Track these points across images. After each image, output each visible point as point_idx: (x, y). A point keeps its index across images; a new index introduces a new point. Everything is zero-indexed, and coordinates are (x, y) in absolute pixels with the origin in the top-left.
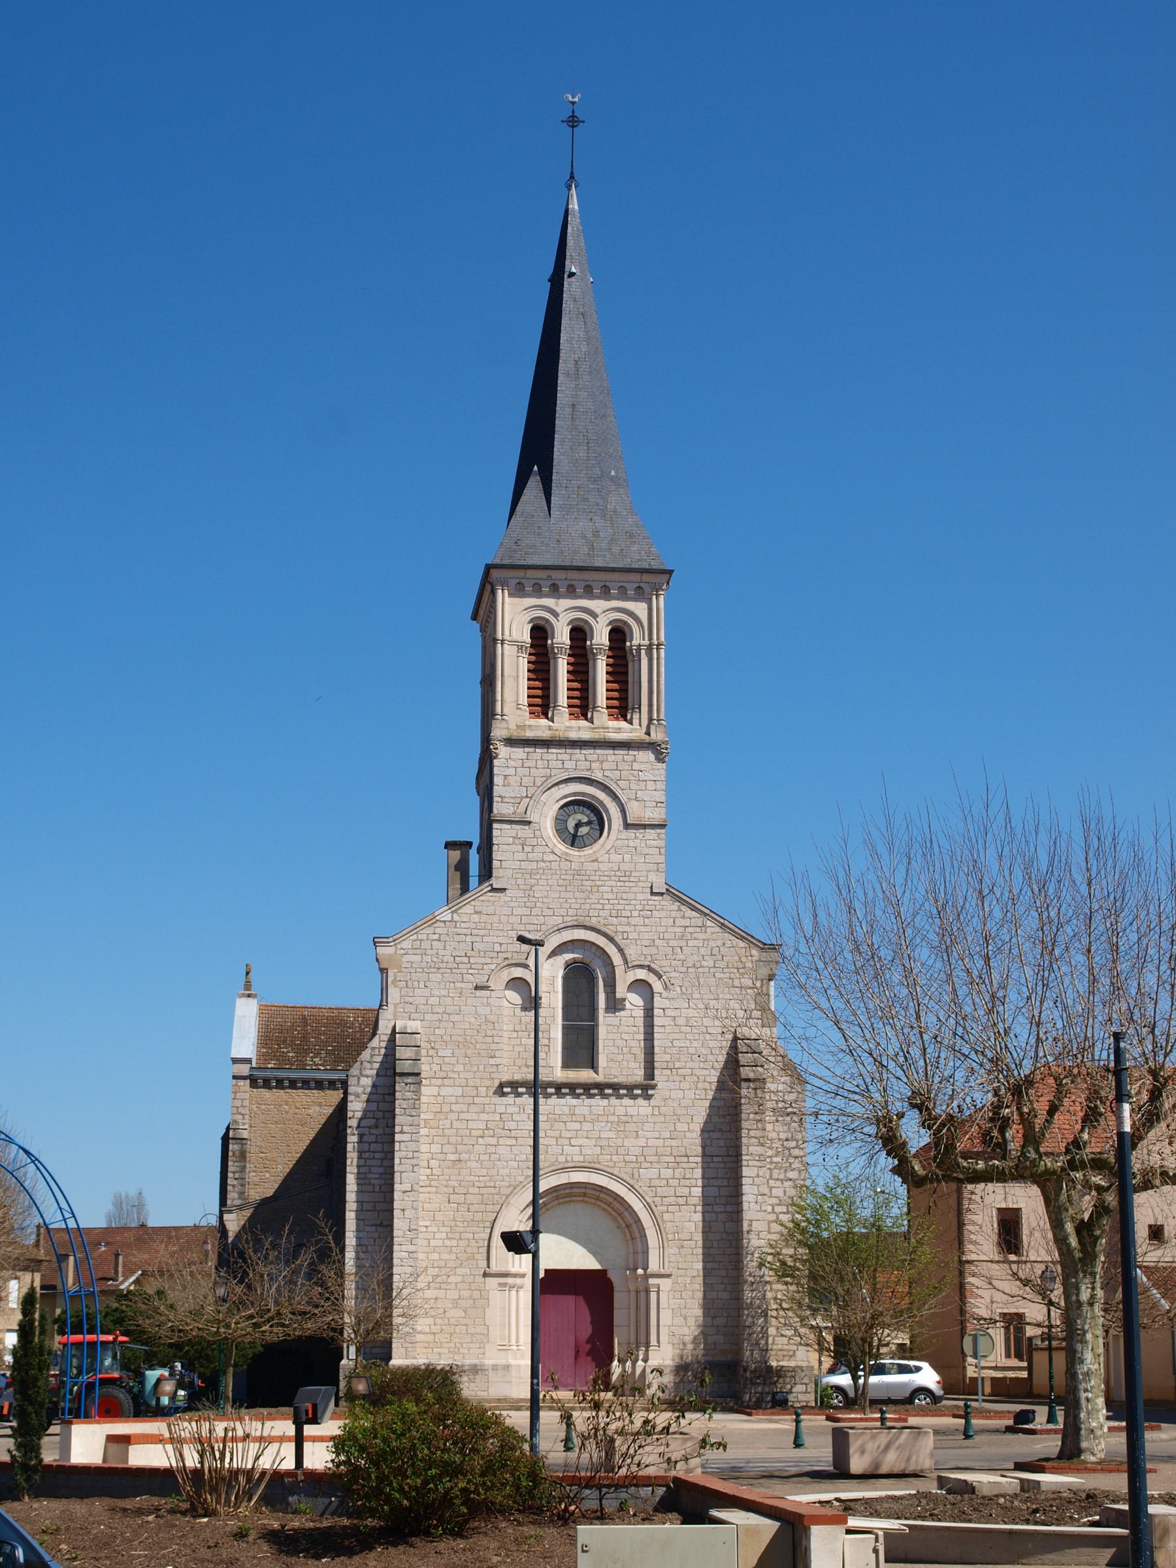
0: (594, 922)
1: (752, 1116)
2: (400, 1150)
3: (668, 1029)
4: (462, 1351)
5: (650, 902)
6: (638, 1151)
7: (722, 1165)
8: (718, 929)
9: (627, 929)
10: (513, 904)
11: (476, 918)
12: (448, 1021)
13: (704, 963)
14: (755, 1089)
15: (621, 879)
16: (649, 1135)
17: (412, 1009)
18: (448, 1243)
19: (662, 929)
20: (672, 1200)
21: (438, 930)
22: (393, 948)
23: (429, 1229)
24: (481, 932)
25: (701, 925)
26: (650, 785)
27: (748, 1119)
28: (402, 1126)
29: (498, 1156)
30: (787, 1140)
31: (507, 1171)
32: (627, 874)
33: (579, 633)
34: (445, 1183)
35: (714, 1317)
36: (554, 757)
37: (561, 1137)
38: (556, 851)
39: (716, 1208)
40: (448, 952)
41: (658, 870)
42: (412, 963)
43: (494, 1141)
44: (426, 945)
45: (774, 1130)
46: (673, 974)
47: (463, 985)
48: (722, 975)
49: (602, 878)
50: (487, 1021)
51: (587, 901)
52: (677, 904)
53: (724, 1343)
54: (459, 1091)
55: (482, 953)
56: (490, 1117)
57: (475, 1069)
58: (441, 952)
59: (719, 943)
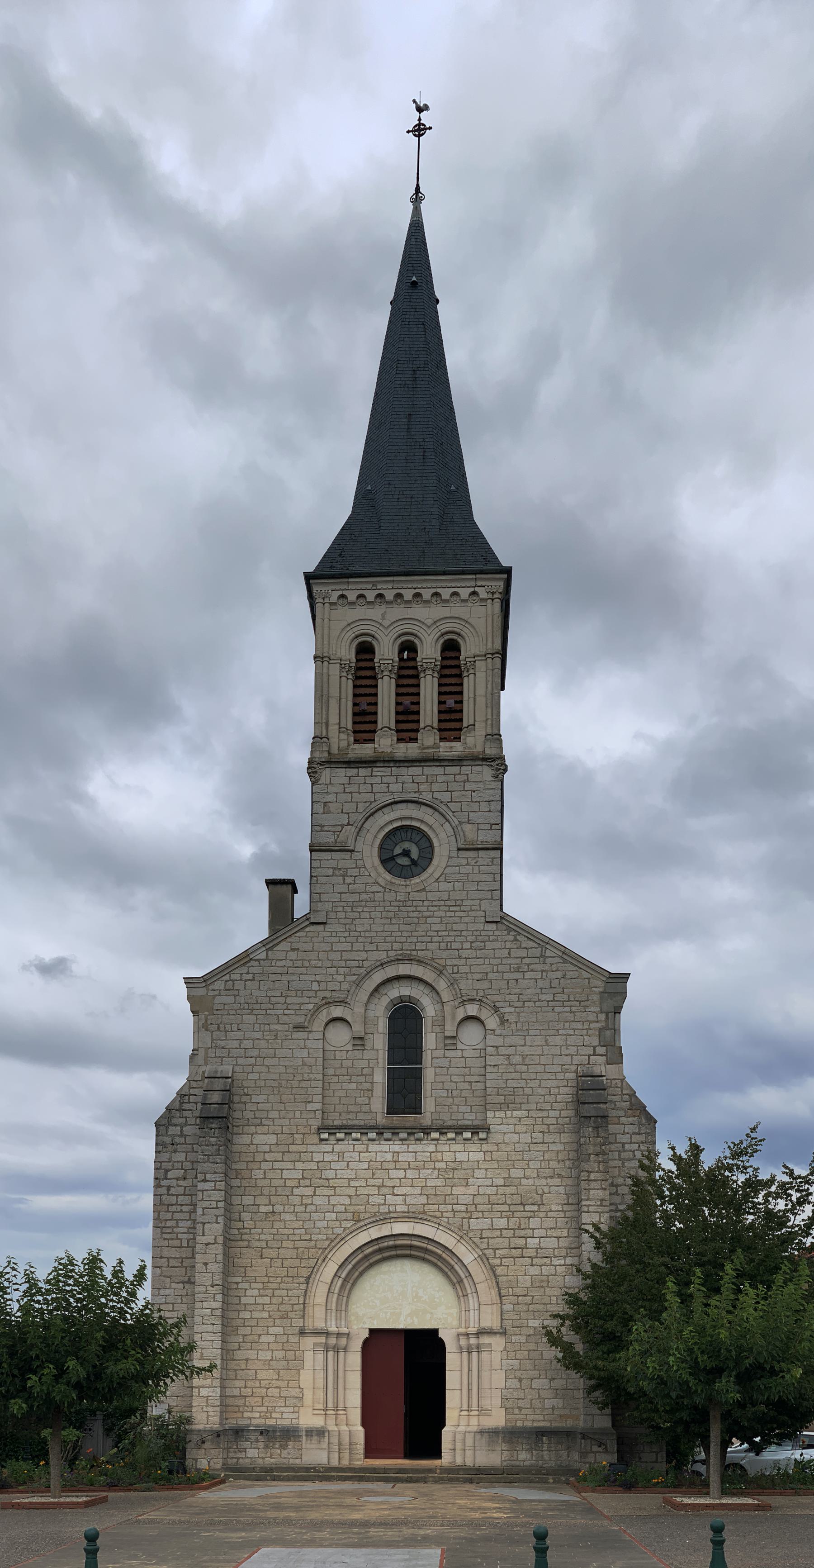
2: (202, 1200)
3: (502, 1069)
5: (483, 933)
8: (558, 960)
9: (455, 962)
11: (293, 955)
12: (263, 1065)
13: (543, 997)
15: (452, 908)
16: (479, 1182)
21: (251, 970)
22: (205, 989)
23: (240, 1286)
26: (484, 807)
28: (205, 1174)
29: (313, 1207)
32: (458, 903)
33: (408, 648)
34: (257, 1237)
36: (378, 780)
37: (383, 1186)
38: (380, 881)
39: (556, 1262)
40: (263, 993)
41: (492, 899)
43: (309, 1191)
45: (619, 1175)
46: (507, 1010)
48: (561, 1009)
50: (304, 1064)
51: (414, 934)
52: (513, 933)
53: (564, 1408)
54: (272, 1139)
55: (299, 993)
56: (306, 1166)
57: (291, 1115)
58: (255, 993)
59: (559, 974)
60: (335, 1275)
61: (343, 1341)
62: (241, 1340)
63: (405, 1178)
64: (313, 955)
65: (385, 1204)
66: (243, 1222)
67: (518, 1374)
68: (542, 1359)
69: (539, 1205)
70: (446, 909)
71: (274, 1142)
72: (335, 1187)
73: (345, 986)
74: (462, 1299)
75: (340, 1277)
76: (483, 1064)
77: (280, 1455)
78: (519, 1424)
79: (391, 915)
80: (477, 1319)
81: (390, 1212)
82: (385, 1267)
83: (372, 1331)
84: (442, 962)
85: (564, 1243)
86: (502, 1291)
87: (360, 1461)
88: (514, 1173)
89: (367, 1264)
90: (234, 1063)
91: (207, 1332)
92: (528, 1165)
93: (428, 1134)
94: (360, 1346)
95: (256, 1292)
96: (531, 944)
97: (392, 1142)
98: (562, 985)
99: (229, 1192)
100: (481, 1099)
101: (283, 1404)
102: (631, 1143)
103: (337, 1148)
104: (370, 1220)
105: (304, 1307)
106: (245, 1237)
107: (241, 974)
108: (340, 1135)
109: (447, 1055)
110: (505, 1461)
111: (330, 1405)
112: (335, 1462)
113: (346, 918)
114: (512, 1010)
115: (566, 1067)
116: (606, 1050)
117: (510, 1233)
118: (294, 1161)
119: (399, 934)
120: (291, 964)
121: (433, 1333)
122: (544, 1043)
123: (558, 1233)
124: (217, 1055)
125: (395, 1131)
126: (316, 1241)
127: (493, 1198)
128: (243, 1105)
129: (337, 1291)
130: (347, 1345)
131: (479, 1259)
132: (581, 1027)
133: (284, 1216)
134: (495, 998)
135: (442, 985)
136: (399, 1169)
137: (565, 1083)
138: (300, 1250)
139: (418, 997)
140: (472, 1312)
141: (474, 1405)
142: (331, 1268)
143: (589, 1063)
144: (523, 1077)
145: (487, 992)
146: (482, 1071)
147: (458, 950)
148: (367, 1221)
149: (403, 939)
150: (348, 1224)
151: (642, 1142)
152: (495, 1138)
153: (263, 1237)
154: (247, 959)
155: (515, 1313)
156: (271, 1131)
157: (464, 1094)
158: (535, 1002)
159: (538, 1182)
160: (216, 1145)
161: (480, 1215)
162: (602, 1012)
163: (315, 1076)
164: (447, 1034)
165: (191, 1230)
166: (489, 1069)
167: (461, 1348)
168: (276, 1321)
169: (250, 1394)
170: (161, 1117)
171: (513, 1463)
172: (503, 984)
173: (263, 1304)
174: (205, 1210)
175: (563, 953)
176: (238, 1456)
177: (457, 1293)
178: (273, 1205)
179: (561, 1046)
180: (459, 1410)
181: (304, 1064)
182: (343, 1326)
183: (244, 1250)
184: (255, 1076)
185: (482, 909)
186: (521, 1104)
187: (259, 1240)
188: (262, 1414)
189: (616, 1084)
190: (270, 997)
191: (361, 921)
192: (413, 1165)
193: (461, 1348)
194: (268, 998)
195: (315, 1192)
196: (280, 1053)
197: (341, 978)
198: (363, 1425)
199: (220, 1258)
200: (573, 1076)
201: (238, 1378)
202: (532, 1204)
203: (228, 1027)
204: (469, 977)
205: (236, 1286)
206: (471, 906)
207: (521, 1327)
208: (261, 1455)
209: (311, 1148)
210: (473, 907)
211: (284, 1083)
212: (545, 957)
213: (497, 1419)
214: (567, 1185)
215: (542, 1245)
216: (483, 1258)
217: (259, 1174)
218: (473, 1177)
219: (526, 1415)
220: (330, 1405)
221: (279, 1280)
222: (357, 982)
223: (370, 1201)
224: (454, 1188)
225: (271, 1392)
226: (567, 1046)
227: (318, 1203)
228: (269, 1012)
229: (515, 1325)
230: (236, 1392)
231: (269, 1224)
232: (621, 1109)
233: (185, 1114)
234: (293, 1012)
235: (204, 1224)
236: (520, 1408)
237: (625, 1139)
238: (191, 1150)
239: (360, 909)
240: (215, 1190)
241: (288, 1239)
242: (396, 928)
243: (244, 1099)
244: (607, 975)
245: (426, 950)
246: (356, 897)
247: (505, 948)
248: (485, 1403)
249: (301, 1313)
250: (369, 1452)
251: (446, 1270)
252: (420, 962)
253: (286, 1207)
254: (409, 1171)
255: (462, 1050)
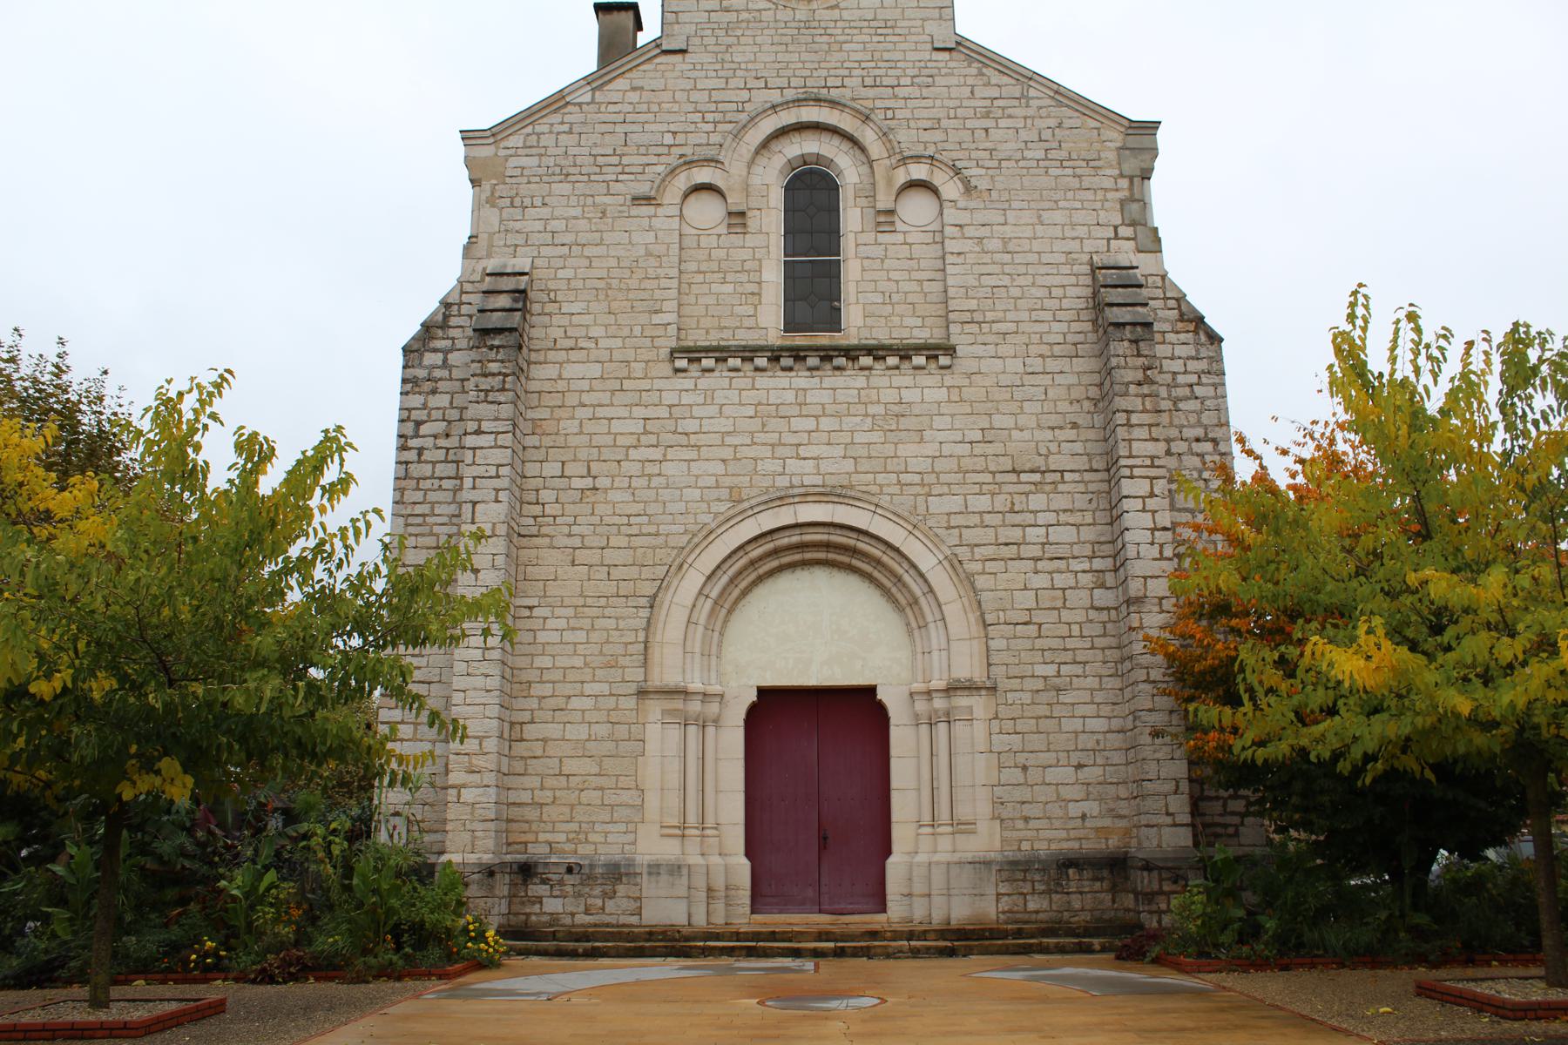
0: (834, 93)
1: (1132, 389)
3: (971, 258)
4: (592, 837)
5: (929, 65)
6: (925, 465)
7: (1081, 488)
8: (1049, 102)
9: (889, 104)
10: (697, 74)
11: (634, 97)
12: (582, 256)
13: (1028, 154)
14: (1135, 342)
15: (879, 31)
16: (941, 436)
17: (520, 240)
18: (569, 636)
19: (952, 103)
20: (989, 551)
21: (567, 118)
22: (492, 148)
23: (536, 612)
24: (642, 118)
25: (1018, 95)
27: (1126, 394)
28: (479, 421)
29: (662, 480)
30: (1198, 440)
31: (681, 506)
32: (889, 24)
34: (566, 530)
35: (1080, 766)
39: (1076, 565)
40: (586, 151)
41: (941, 18)
42: (523, 168)
43: (656, 454)
44: (547, 140)
45: (1171, 424)
47: (608, 199)
49: (847, 31)
51: (822, 65)
52: (976, 65)
54: (595, 370)
57: (626, 332)
58: (571, 151)
59: (1052, 122)
60: (700, 593)
61: (714, 708)
62: (535, 706)
63: (817, 430)
64: (667, 96)
65: (783, 474)
66: (543, 504)
67: (1021, 759)
68: (1060, 731)
69: (1043, 472)
70: (873, 31)
71: (598, 375)
72: (699, 447)
73: (715, 138)
74: (916, 632)
75: (707, 597)
76: (940, 253)
77: (603, 908)
78: (1026, 846)
79: (788, 39)
80: (945, 666)
81: (792, 487)
82: (786, 581)
83: (763, 692)
84: (869, 104)
85: (1088, 534)
86: (987, 616)
87: (743, 917)
88: (999, 420)
89: (753, 576)
90: (536, 254)
91: (475, 689)
92: (1021, 408)
93: (854, 359)
94: (743, 715)
95: (562, 623)
96: (1006, 80)
97: (793, 374)
98: (1058, 138)
99: (520, 453)
100: (939, 306)
101: (608, 819)
102: (1185, 372)
103: (706, 382)
104: (759, 499)
105: (646, 648)
106: (544, 530)
107: (552, 125)
108: (708, 363)
109: (879, 240)
110: (1004, 912)
111: (692, 819)
112: (700, 921)
113: (717, 44)
114: (983, 171)
115: (1073, 256)
116: (1135, 232)
117: (994, 520)
118: (631, 405)
119: (801, 65)
120: (630, 108)
121: (867, 693)
122: (1036, 221)
123: (1076, 518)
124: (508, 243)
125: (798, 354)
126: (667, 535)
127: (967, 463)
128: (548, 318)
129: (702, 620)
130: (719, 715)
131: (945, 563)
132: (1092, 198)
133: (614, 496)
134: (955, 155)
135: (868, 136)
136: (806, 416)
137: (1073, 280)
138: (640, 551)
139: (831, 156)
140: (935, 654)
141: (944, 815)
142: (693, 581)
143: (1108, 251)
144: (1007, 271)
145: (940, 146)
146: (939, 264)
147: (893, 87)
148: (753, 502)
149: (808, 73)
150: (723, 507)
151: (1204, 372)
152: (964, 364)
153: (575, 530)
154: (563, 102)
155: (1011, 653)
156: (592, 358)
157: (911, 298)
158: (1017, 161)
159: (1039, 435)
160: (499, 374)
161: (945, 489)
162: (1122, 176)
163: (667, 271)
164: (881, 206)
165: (455, 520)
166: (950, 259)
167: (917, 716)
168: (598, 672)
169: (549, 801)
170: (413, 338)
171: (1018, 916)
172: (966, 135)
173: (575, 644)
174: (477, 480)
175: (1056, 92)
176: (528, 911)
177: (908, 624)
178: (595, 477)
179: (1063, 225)
180: (915, 825)
181: (649, 254)
182: (713, 682)
183: (543, 553)
184: (569, 273)
185: (927, 32)
186: (1005, 311)
187: (570, 535)
188: (572, 836)
189: (1154, 282)
190: (595, 156)
191: (740, 49)
192: (830, 409)
193: (917, 716)
194: (592, 159)
195: (665, 455)
196: (609, 237)
197: (710, 127)
198: (748, 854)
199: (500, 560)
200: (1086, 269)
201: (530, 771)
202: (1032, 471)
203: (527, 202)
204: (912, 124)
205: (527, 613)
206: (910, 28)
207: (1022, 677)
208: (569, 909)
209: (658, 384)
210: (913, 30)
211: (615, 283)
212: (1028, 99)
213: (986, 841)
214: (1087, 441)
215: (1051, 539)
216: (954, 563)
217: (571, 426)
218: (932, 429)
219: (1037, 830)
220: (692, 819)
221: (603, 601)
222: (735, 132)
223: (759, 468)
224: (900, 446)
225: (586, 797)
226: (1073, 225)
227: (670, 473)
228: (593, 177)
229: (1011, 675)
230: (525, 797)
231: (587, 509)
232: (1166, 320)
233: (452, 333)
234: (632, 177)
235: (475, 503)
236: (1026, 819)
237: (1177, 366)
238: (460, 390)
239: (739, 32)
240: (496, 447)
241: (619, 533)
242: (795, 57)
243: (550, 308)
244: (1126, 123)
245: (843, 86)
246: (733, 17)
247: (965, 85)
248: (963, 812)
249: (642, 657)
250: (760, 898)
251: (888, 584)
252: (834, 104)
253: (617, 479)
254: (822, 420)
255: (905, 233)
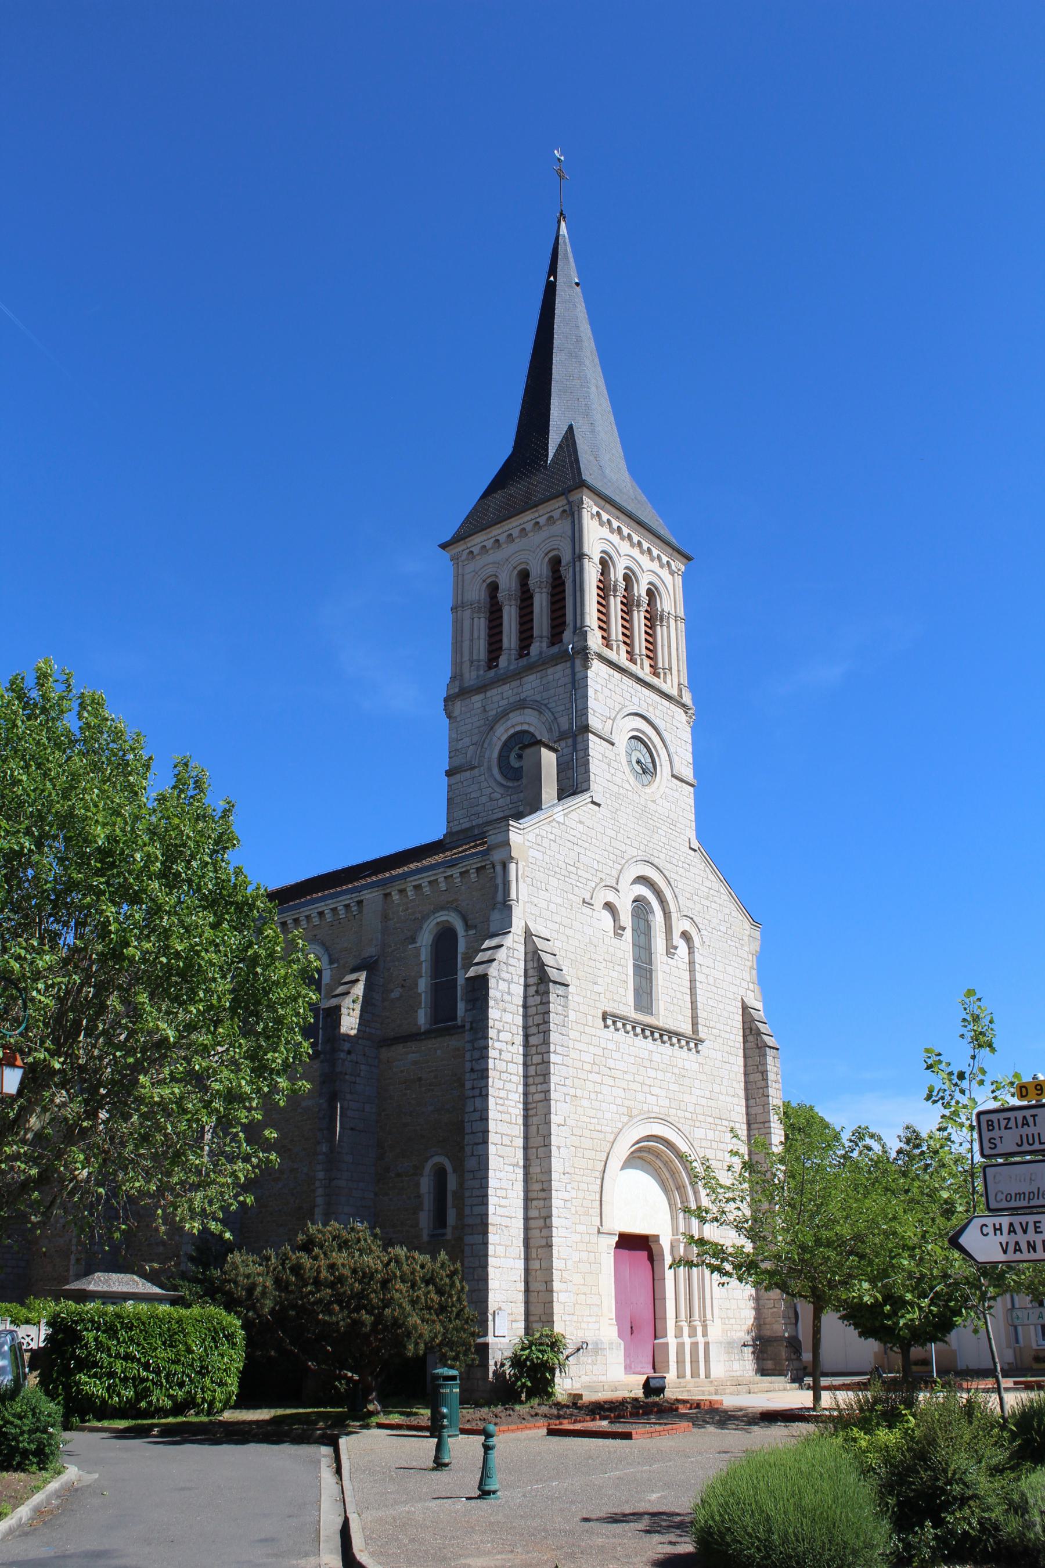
8: (726, 898)
44: (546, 843)
52: (703, 864)
